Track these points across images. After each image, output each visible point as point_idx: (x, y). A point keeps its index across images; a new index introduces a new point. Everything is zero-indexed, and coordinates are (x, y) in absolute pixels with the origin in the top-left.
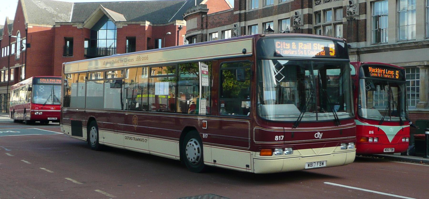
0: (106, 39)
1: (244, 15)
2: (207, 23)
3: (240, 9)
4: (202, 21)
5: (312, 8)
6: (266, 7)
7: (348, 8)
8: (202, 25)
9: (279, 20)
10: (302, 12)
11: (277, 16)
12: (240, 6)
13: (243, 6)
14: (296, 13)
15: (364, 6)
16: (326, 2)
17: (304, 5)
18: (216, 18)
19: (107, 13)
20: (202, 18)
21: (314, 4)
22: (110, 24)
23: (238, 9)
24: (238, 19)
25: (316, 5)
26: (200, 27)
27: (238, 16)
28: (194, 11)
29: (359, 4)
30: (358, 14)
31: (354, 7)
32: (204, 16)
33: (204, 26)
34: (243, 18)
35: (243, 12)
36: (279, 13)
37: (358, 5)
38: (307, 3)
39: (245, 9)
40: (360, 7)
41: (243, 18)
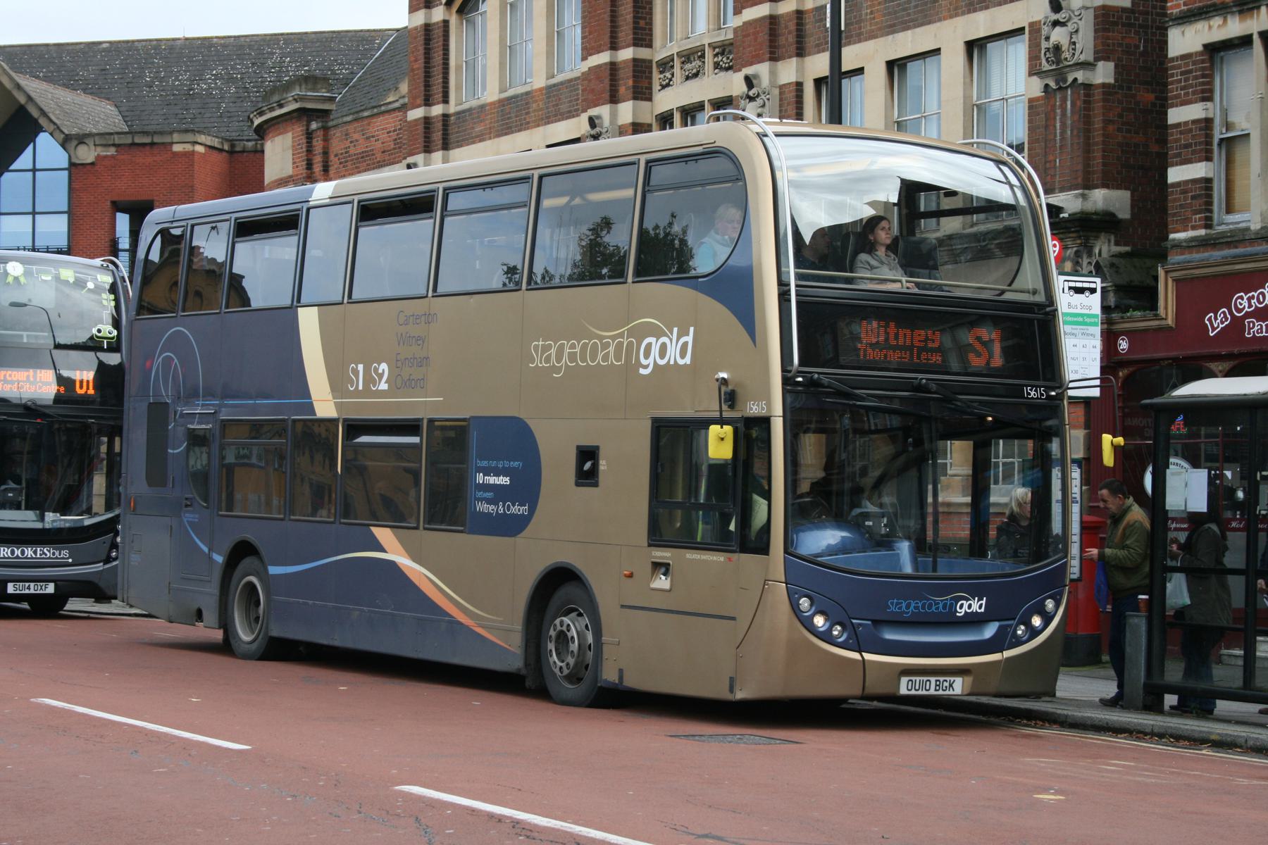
0: (34, 213)
1: (439, 125)
2: (326, 153)
3: (428, 102)
4: (309, 150)
5: (650, 99)
6: (510, 93)
7: (1045, 30)
8: (309, 165)
9: (890, 65)
10: (773, 74)
11: (541, 128)
12: (427, 86)
13: (437, 90)
14: (592, 122)
15: (791, 96)
16: (688, 78)
17: (622, 90)
18: (356, 136)
19: (30, 98)
20: (309, 136)
21: (656, 86)
22: (47, 149)
23: (420, 100)
24: (421, 140)
25: (663, 87)
26: (302, 170)
27: (421, 128)
28: (281, 106)
29: (781, 87)
30: (1088, 56)
31: (759, 102)
32: (314, 126)
33: (318, 168)
34: (437, 136)
35: (437, 110)
36: (548, 119)
37: (777, 92)
38: (630, 83)
39: (446, 100)
40: (781, 100)
41: (437, 136)
